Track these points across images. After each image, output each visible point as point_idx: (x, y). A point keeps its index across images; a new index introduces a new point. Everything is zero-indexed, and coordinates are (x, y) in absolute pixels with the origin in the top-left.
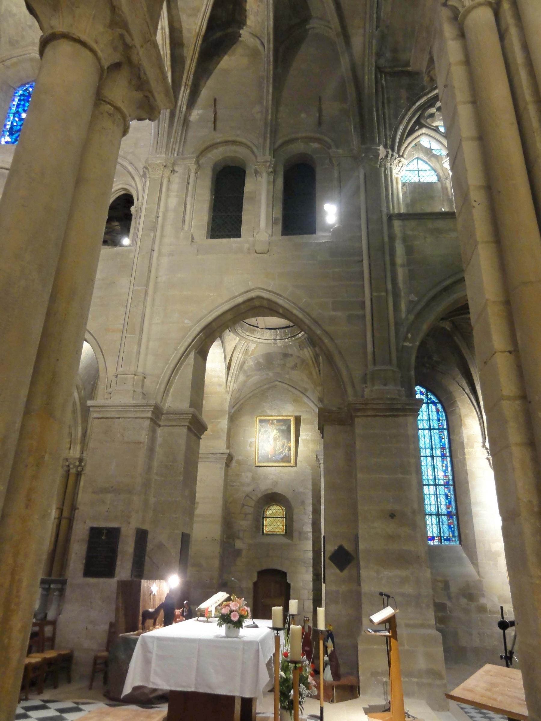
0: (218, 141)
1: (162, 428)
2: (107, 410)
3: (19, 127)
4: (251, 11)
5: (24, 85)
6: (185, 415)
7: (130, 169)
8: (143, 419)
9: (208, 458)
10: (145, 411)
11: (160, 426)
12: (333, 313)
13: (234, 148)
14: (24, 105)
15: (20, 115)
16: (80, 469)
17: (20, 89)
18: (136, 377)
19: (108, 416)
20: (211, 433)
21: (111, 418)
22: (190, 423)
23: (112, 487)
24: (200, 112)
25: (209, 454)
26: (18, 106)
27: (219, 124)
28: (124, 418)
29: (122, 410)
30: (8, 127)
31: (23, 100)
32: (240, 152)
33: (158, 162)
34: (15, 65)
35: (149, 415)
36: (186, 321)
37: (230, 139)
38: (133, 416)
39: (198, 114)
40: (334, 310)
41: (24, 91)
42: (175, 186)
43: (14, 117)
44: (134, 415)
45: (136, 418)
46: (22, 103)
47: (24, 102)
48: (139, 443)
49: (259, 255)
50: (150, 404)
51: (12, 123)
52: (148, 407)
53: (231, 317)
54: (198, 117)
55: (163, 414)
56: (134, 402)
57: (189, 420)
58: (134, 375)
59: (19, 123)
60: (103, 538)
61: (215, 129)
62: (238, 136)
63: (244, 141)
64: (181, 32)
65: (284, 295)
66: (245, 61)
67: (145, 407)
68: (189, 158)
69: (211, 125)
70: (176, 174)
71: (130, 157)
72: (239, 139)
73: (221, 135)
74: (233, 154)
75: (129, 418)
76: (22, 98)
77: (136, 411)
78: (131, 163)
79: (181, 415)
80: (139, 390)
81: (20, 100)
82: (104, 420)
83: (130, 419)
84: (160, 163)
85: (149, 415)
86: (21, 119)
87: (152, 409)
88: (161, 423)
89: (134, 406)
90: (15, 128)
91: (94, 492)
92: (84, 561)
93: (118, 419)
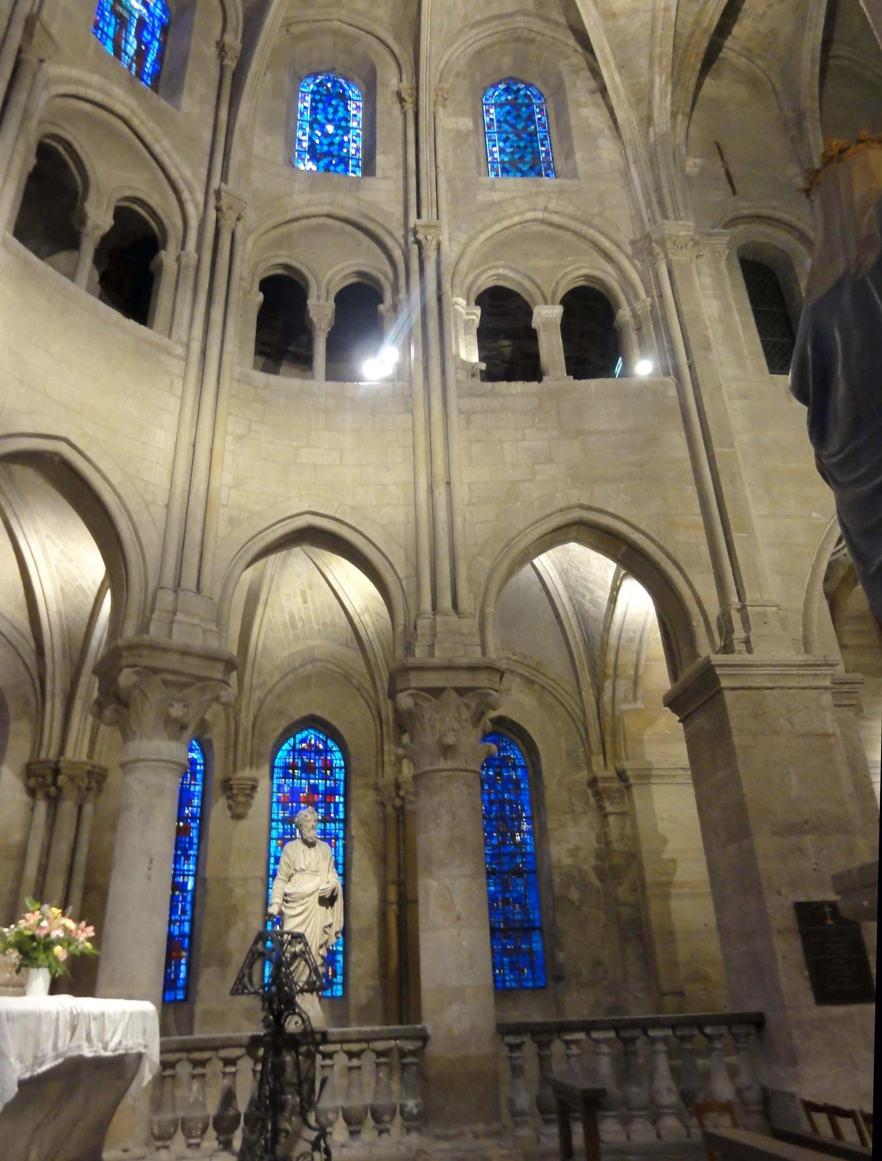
0: (746, 212)
2: (752, 672)
3: (325, 148)
4: (750, 11)
5: (316, 76)
6: (848, 686)
7: (605, 243)
8: (816, 691)
9: (675, 776)
10: (820, 675)
13: (763, 228)
14: (325, 110)
15: (322, 127)
16: (398, 802)
17: (309, 81)
18: (779, 611)
19: (750, 684)
20: (668, 732)
21: (757, 688)
23: (807, 822)
24: (698, 161)
25: (676, 769)
26: (314, 110)
27: (738, 187)
28: (782, 688)
29: (778, 672)
30: (305, 145)
31: (320, 101)
32: (780, 238)
33: (682, 233)
34: (304, 36)
36: (814, 515)
37: (764, 212)
38: (796, 685)
39: (695, 165)
41: (318, 85)
42: (708, 281)
43: (312, 128)
44: (799, 683)
45: (804, 688)
46: (320, 106)
47: (324, 104)
48: (828, 735)
50: (830, 662)
51: (310, 139)
52: (827, 668)
54: (697, 170)
58: (775, 608)
59: (326, 141)
60: (830, 922)
61: (734, 192)
62: (774, 208)
63: (787, 217)
66: (742, 92)
67: (818, 668)
68: (720, 234)
69: (724, 184)
70: (700, 259)
71: (596, 221)
72: (777, 214)
73: (748, 204)
74: (763, 240)
75: (790, 688)
76: (318, 97)
77: (803, 675)
78: (603, 233)
79: (843, 686)
81: (313, 100)
82: (744, 691)
83: (793, 691)
84: (687, 236)
86: (325, 135)
89: (801, 666)
90: (318, 147)
91: (775, 833)
92: (807, 974)
93: (770, 691)
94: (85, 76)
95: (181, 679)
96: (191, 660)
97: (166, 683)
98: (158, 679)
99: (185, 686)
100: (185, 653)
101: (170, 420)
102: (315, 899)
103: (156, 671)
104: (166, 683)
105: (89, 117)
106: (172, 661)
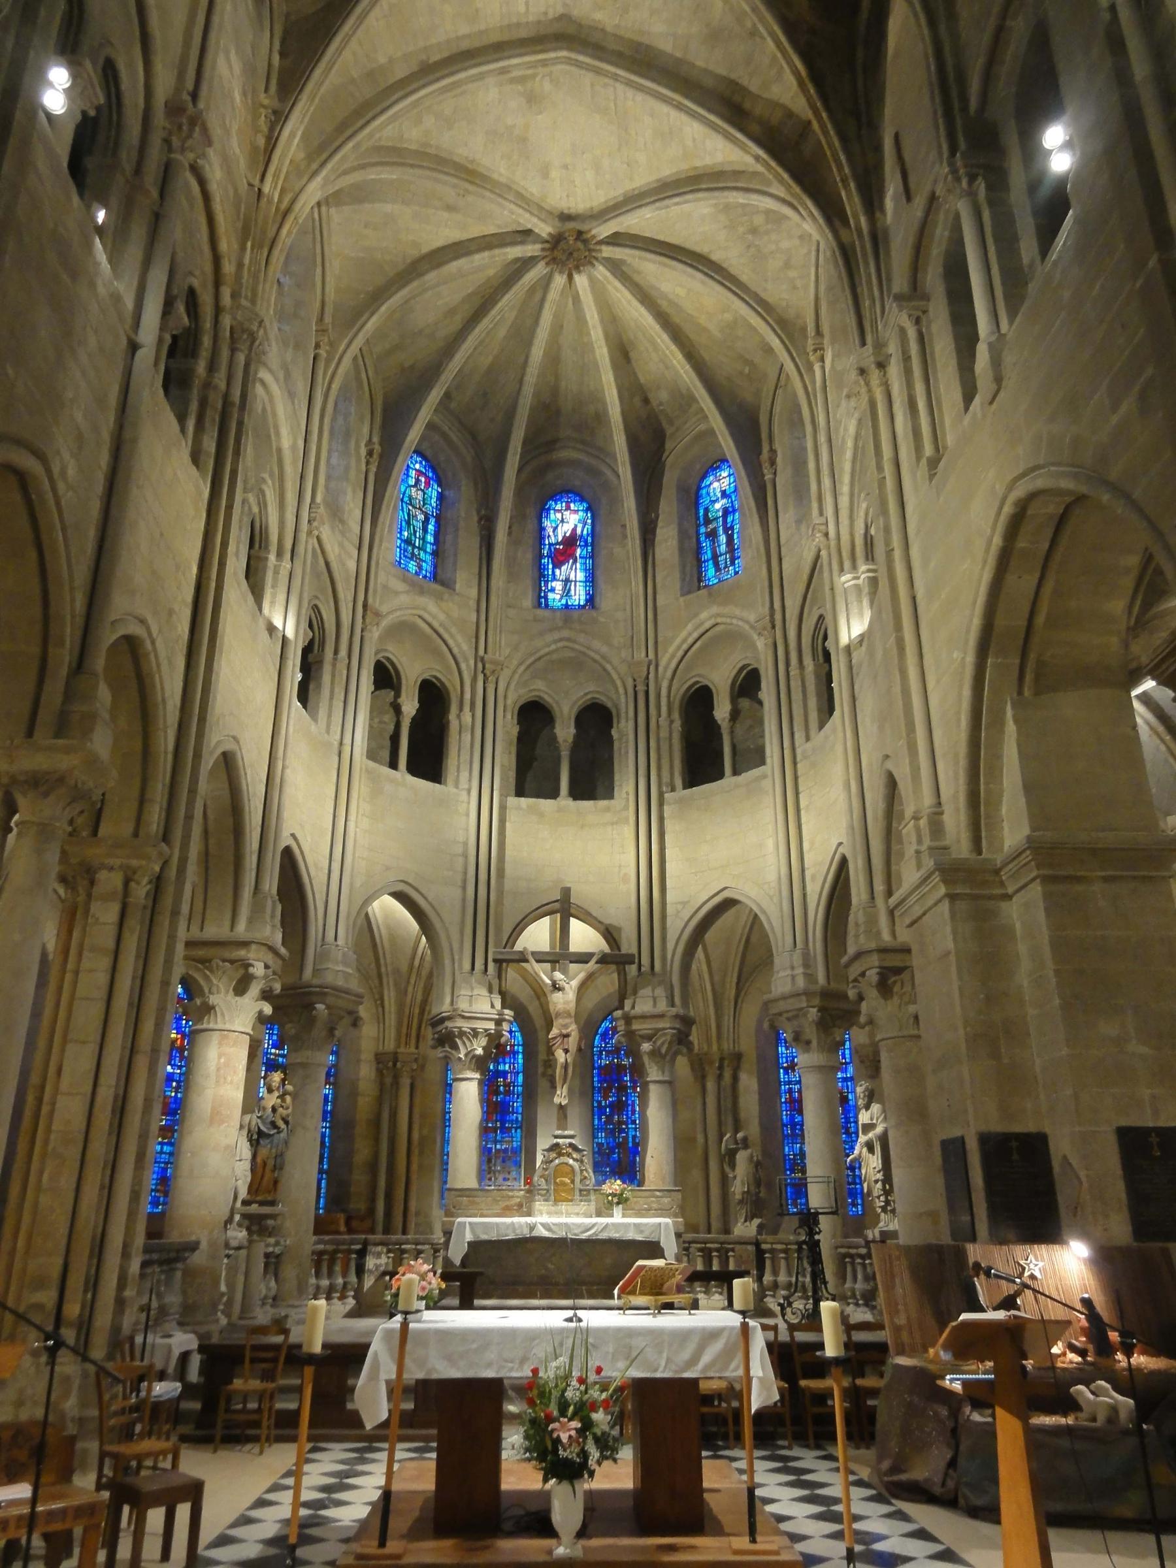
1: (1014, 899)
11: (1008, 897)
12: (1115, 419)
22: (1038, 867)
35: (942, 890)
40: (1115, 408)
49: (995, 405)
53: (1031, 580)
55: (997, 872)
56: (919, 875)
57: (1033, 863)
64: (790, 114)
65: (1042, 462)
80: (927, 842)
85: (942, 890)
87: (936, 878)
88: (1010, 890)
94: (684, 634)
95: (790, 1014)
96: (791, 1001)
97: (788, 1019)
98: (783, 1018)
99: (796, 1016)
100: (784, 998)
101: (771, 827)
102: (865, 1150)
103: (780, 1014)
104: (788, 1019)
105: (701, 649)
106: (782, 1006)
